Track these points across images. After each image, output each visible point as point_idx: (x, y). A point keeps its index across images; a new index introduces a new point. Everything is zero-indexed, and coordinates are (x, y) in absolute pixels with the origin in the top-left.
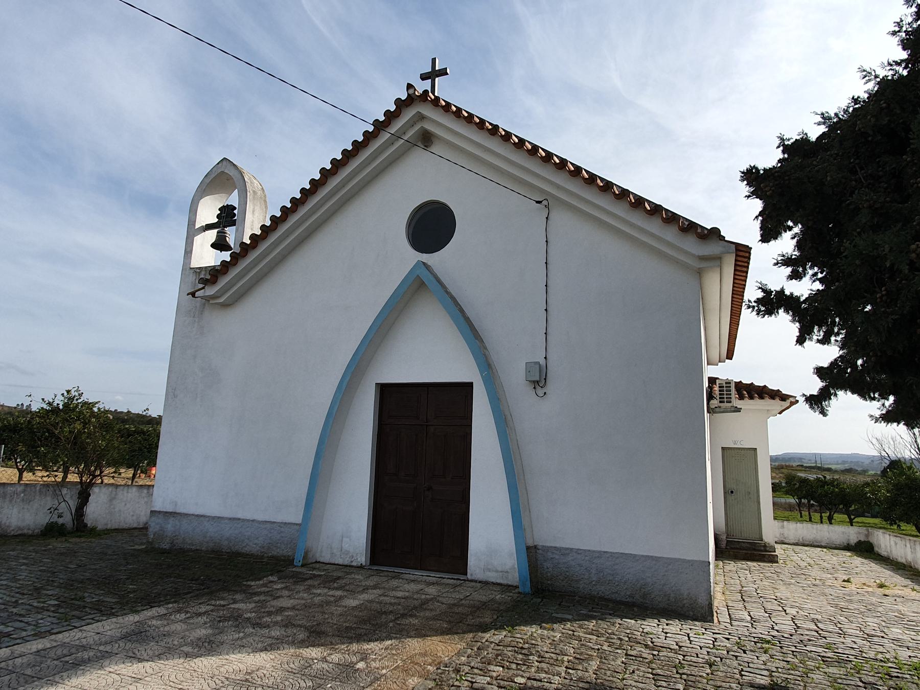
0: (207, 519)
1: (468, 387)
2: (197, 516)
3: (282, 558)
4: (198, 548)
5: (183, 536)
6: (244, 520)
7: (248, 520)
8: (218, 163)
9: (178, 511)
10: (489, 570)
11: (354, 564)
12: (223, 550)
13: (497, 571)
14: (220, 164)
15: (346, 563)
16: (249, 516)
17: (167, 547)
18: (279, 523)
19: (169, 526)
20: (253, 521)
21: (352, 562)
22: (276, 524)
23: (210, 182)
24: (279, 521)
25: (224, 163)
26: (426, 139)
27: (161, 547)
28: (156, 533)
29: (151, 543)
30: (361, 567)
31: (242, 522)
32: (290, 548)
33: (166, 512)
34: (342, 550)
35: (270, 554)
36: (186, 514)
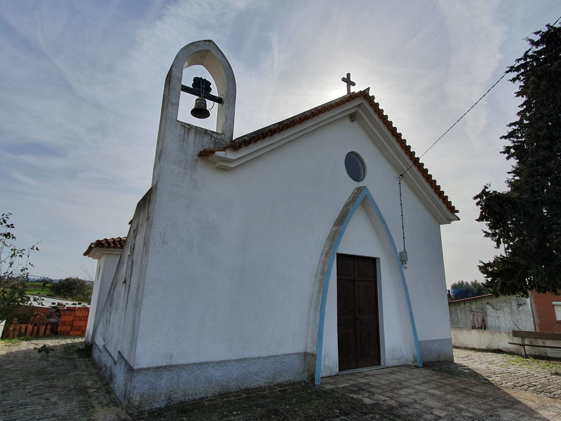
0: (212, 365)
1: (373, 261)
2: (200, 364)
3: (285, 383)
4: (203, 395)
5: (183, 388)
6: (250, 359)
7: (254, 359)
8: (205, 41)
9: (174, 363)
10: (394, 359)
11: (333, 374)
12: (231, 391)
13: (397, 359)
14: (207, 43)
15: (328, 375)
16: (254, 355)
17: (163, 405)
18: (281, 355)
19: (164, 381)
20: (258, 358)
21: (331, 373)
22: (278, 357)
23: (196, 52)
24: (280, 354)
25: (211, 44)
26: (353, 117)
27: (154, 407)
28: (143, 394)
29: (139, 407)
30: (337, 375)
31: (249, 361)
32: (291, 374)
33: (158, 368)
34: (325, 366)
35: (276, 383)
36: (186, 365)
